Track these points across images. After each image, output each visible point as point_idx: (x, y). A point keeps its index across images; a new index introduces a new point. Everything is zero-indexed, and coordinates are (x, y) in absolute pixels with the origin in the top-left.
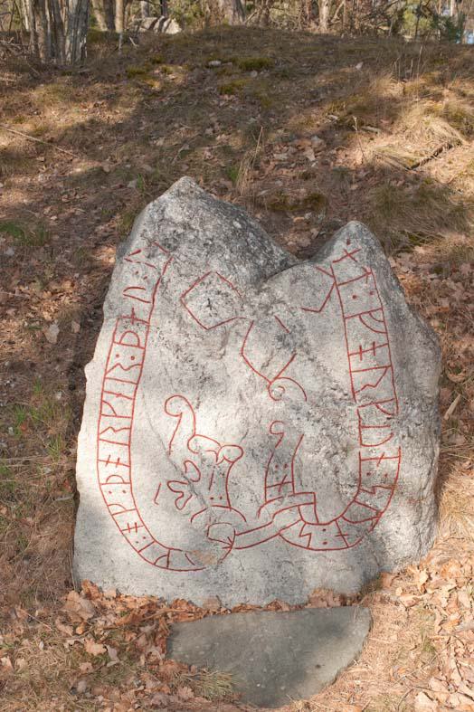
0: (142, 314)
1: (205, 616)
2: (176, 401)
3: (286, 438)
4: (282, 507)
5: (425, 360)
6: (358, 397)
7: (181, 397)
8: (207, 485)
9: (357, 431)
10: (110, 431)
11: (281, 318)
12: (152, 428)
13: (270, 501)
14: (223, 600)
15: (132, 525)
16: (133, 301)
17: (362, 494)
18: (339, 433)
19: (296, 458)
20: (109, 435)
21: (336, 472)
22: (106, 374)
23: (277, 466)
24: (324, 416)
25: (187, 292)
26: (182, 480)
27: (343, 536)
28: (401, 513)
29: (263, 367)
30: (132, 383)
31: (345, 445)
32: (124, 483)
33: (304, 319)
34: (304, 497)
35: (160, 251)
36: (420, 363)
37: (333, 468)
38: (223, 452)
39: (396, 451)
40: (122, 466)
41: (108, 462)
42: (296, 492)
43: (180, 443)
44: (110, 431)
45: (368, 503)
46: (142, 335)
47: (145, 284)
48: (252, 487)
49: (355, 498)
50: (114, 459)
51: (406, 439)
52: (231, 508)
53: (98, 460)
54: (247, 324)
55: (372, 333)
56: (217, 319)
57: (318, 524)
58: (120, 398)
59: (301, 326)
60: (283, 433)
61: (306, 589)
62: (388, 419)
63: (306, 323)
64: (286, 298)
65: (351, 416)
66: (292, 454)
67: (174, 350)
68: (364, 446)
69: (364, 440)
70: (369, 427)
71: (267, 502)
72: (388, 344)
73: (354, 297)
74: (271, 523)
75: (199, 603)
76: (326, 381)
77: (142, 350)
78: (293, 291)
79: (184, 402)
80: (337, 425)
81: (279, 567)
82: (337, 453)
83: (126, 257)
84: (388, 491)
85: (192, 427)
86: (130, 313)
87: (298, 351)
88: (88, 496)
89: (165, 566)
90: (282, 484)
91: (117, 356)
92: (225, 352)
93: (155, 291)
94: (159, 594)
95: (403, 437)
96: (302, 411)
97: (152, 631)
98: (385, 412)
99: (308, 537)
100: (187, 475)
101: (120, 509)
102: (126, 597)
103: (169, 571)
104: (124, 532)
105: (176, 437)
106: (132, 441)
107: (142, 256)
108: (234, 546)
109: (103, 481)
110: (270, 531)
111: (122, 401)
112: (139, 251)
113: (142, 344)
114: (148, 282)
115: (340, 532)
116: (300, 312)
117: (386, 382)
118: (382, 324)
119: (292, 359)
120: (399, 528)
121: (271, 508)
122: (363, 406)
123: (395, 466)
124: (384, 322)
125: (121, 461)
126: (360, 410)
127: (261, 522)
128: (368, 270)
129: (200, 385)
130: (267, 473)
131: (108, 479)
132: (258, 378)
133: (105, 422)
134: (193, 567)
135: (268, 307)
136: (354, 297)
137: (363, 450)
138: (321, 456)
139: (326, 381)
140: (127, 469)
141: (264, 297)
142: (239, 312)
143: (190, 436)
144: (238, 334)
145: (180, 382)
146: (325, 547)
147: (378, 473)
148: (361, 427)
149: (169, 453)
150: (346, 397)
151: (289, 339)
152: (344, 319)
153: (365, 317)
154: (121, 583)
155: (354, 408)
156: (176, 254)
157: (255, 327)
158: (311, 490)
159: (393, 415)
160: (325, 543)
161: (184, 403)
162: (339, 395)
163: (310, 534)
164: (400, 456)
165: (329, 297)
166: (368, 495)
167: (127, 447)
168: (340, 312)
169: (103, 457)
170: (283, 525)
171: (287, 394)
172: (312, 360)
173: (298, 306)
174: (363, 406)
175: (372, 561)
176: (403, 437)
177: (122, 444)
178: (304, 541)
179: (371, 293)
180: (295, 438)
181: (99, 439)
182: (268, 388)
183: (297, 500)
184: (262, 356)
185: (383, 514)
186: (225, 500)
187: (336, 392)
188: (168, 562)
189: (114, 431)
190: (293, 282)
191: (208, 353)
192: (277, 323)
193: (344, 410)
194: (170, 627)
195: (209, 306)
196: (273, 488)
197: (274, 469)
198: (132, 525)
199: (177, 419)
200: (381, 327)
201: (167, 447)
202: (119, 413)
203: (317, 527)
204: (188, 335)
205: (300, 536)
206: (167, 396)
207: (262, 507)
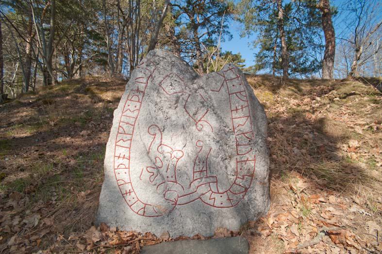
0: (142, 88)
1: (160, 243)
2: (154, 128)
4: (201, 183)
5: (263, 118)
6: (236, 131)
8: (165, 170)
9: (236, 147)
10: (121, 141)
11: (202, 94)
12: (141, 140)
13: (196, 180)
14: (171, 233)
15: (128, 191)
16: (139, 84)
17: (238, 179)
18: (227, 148)
19: (208, 159)
20: (121, 143)
21: (226, 168)
22: (123, 113)
23: (199, 162)
26: (154, 166)
27: (230, 200)
30: (134, 118)
31: (230, 154)
34: (211, 179)
35: (152, 64)
36: (260, 120)
38: (174, 154)
39: (253, 157)
40: (126, 159)
41: (119, 157)
43: (154, 148)
45: (241, 184)
46: (141, 97)
47: (144, 75)
51: (257, 152)
53: (115, 156)
54: (187, 95)
55: (241, 101)
56: (175, 91)
57: (218, 193)
58: (128, 125)
59: (210, 98)
60: (202, 146)
61: (213, 228)
62: (249, 141)
63: (213, 96)
64: (204, 86)
65: (233, 140)
66: (206, 157)
68: (239, 155)
69: (239, 152)
71: (194, 180)
73: (233, 86)
74: (196, 191)
75: (158, 235)
76: (222, 123)
79: (157, 128)
80: (227, 145)
81: (200, 215)
82: (226, 159)
83: (138, 66)
84: (250, 178)
85: (160, 141)
86: (137, 89)
87: (209, 109)
88: (108, 176)
90: (201, 171)
91: (129, 106)
93: (148, 79)
94: (139, 230)
96: (211, 137)
97: (130, 249)
98: (248, 138)
99: (213, 200)
100: (156, 164)
101: (123, 182)
102: (121, 231)
103: (144, 217)
106: (131, 146)
107: (144, 66)
108: (177, 203)
109: (116, 167)
110: (195, 196)
111: (128, 127)
113: (140, 101)
116: (210, 92)
117: (248, 123)
119: (207, 112)
120: (258, 196)
121: (196, 183)
123: (253, 165)
124: (246, 96)
125: (125, 156)
126: (237, 136)
127: (191, 190)
129: (165, 121)
131: (118, 166)
132: (191, 119)
133: (120, 136)
134: (157, 215)
135: (196, 90)
136: (233, 86)
137: (238, 157)
138: (219, 159)
141: (195, 86)
142: (184, 90)
143: (159, 145)
144: (183, 99)
145: (156, 119)
146: (222, 206)
147: (246, 168)
148: (237, 145)
149: (148, 153)
151: (205, 103)
153: (238, 94)
155: (234, 136)
156: (159, 66)
157: (191, 96)
160: (222, 204)
162: (227, 130)
163: (214, 198)
165: (223, 85)
166: (241, 180)
167: (128, 149)
168: (227, 91)
169: (117, 155)
170: (201, 192)
171: (204, 129)
172: (215, 114)
173: (209, 89)
175: (244, 214)
178: (211, 202)
179: (240, 85)
180: (208, 149)
181: (116, 145)
182: (196, 125)
183: (208, 180)
185: (248, 190)
186: (174, 178)
187: (226, 128)
188: (144, 212)
189: (124, 141)
192: (200, 96)
193: (229, 137)
194: (141, 248)
195: (171, 85)
197: (198, 163)
198: (128, 191)
199: (154, 136)
200: (245, 99)
201: (148, 149)
202: (126, 133)
204: (161, 98)
205: (210, 199)
206: (149, 125)
207: (192, 183)
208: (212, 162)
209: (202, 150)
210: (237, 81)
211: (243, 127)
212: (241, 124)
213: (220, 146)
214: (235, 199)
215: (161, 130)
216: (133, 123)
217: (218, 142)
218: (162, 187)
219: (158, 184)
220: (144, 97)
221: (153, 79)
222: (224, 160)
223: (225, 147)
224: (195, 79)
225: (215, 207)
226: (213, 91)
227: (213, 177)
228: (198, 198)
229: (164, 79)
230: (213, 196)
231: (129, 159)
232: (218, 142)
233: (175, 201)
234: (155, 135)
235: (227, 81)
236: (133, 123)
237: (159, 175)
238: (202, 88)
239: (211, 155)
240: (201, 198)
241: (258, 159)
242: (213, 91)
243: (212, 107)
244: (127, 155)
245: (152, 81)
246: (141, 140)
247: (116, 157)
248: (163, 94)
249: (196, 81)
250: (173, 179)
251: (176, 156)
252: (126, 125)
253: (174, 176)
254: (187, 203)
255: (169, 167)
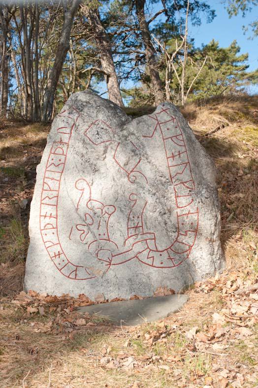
2: (81, 182)
3: (138, 202)
4: (137, 240)
5: (207, 165)
6: (174, 180)
7: (84, 179)
8: (97, 226)
9: (175, 199)
11: (133, 141)
12: (69, 196)
13: (131, 236)
15: (57, 253)
16: (61, 134)
17: (180, 236)
18: (166, 201)
19: (144, 214)
20: (47, 201)
22: (47, 168)
23: (133, 217)
24: (157, 192)
25: (87, 129)
26: (84, 223)
27: (171, 259)
28: (202, 246)
29: (125, 165)
30: (59, 172)
31: (169, 208)
32: (54, 228)
33: (144, 142)
34: (148, 235)
35: (74, 111)
37: (163, 221)
38: (105, 209)
41: (45, 216)
42: (144, 232)
44: (47, 199)
46: (65, 148)
48: (120, 229)
49: (177, 239)
50: (48, 215)
52: (110, 241)
54: (116, 144)
56: (102, 140)
57: (157, 251)
59: (143, 145)
60: (136, 200)
64: (135, 132)
67: (80, 156)
69: (178, 204)
70: (181, 196)
71: (129, 237)
72: (186, 151)
73: (168, 129)
77: (65, 156)
78: (138, 127)
80: (164, 197)
82: (165, 214)
84: (194, 233)
85: (89, 196)
86: (59, 140)
87: (142, 158)
89: (74, 277)
90: (136, 227)
91: (53, 159)
92: (105, 157)
93: (72, 128)
95: (199, 202)
96: (145, 189)
98: (188, 187)
101: (51, 244)
104: (53, 258)
105: (81, 200)
106: (58, 203)
107: (66, 113)
108: (112, 263)
109: (42, 228)
110: (131, 254)
111: (54, 182)
112: (65, 111)
113: (65, 154)
114: (69, 124)
115: (169, 256)
116: (142, 138)
117: (187, 171)
118: (182, 142)
122: (177, 185)
127: (126, 248)
128: (174, 117)
130: (128, 220)
132: (122, 170)
133: (45, 194)
134: (89, 276)
135: (126, 137)
136: (168, 129)
137: (178, 210)
138: (156, 214)
139: (157, 173)
140: (56, 219)
141: (125, 132)
142: (112, 138)
146: (162, 266)
148: (177, 197)
149: (77, 209)
150: (168, 180)
152: (164, 139)
153: (174, 139)
154: (50, 290)
155: (172, 187)
157: (120, 145)
158: (152, 231)
159: (192, 189)
160: (162, 263)
161: (85, 182)
163: (153, 257)
164: (198, 213)
165: (155, 129)
166: (183, 237)
167: (55, 207)
168: (161, 136)
172: (150, 162)
174: (177, 185)
176: (199, 202)
177: (53, 205)
178: (150, 261)
179: (176, 127)
181: (41, 203)
183: (145, 237)
184: (124, 159)
185: (193, 248)
186: (106, 236)
187: (162, 178)
188: (76, 275)
189: (50, 199)
190: (138, 124)
191: (97, 157)
192: (131, 144)
195: (98, 134)
196: (132, 229)
197: (132, 219)
200: (182, 143)
201: (76, 206)
203: (157, 252)
204: (87, 149)
205: (148, 258)
206: (77, 180)
208: (149, 217)
209: (137, 203)
210: (172, 124)
211: (182, 175)
212: (179, 172)
213: (157, 199)
214: (178, 258)
215: (90, 184)
216: (59, 179)
217: (154, 194)
218: (94, 245)
219: (89, 243)
220: (69, 149)
221: (77, 128)
222: (162, 215)
223: (162, 200)
224: (125, 124)
225: (155, 267)
226: (145, 137)
227: (150, 233)
228: (134, 257)
229: (89, 127)
230: (151, 254)
231: (57, 218)
232: (154, 194)
233: (109, 261)
234: (83, 190)
235: (161, 125)
236: (59, 179)
237: (90, 232)
238: (133, 134)
239: (146, 209)
240: (137, 257)
241: (202, 211)
242: (145, 137)
243: (146, 156)
244: (54, 214)
245: (76, 131)
246: (69, 196)
247: (41, 217)
248: (89, 144)
249: (125, 127)
250: (106, 237)
251: (107, 212)
252: (51, 181)
253: (106, 234)
254: (122, 263)
255: (101, 224)
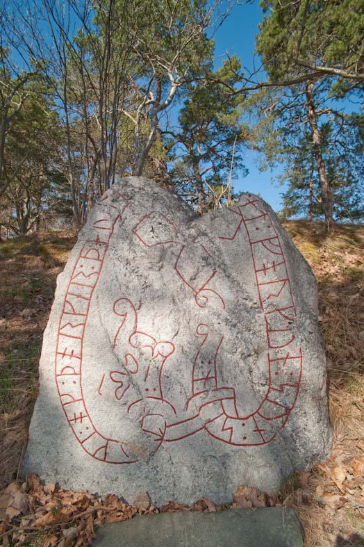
1: (133, 516)
3: (209, 338)
4: (206, 401)
5: (310, 284)
6: (265, 305)
7: (127, 299)
8: (143, 377)
9: (266, 334)
10: (69, 326)
11: (204, 245)
12: (102, 325)
13: (198, 394)
14: (152, 496)
15: (78, 415)
16: (99, 230)
17: (272, 392)
18: (251, 336)
19: (217, 357)
21: (250, 372)
23: (202, 362)
24: (239, 322)
25: (138, 224)
26: (123, 370)
27: (260, 431)
28: (307, 410)
29: (191, 279)
30: (90, 286)
31: (256, 348)
32: (75, 374)
33: (221, 246)
34: (225, 392)
35: (121, 198)
37: (247, 368)
38: (158, 348)
39: (298, 351)
41: (64, 354)
42: (218, 387)
43: (123, 337)
44: (69, 326)
45: (278, 400)
46: (102, 251)
48: (181, 380)
49: (267, 395)
50: (69, 352)
51: (304, 342)
52: (163, 400)
53: (57, 353)
54: (179, 246)
55: (272, 255)
56: (158, 240)
57: (238, 418)
58: (79, 299)
60: (207, 334)
61: (230, 486)
63: (223, 248)
64: (208, 231)
65: (260, 322)
66: (215, 353)
67: (124, 263)
69: (271, 343)
70: (275, 331)
71: (194, 395)
72: (284, 262)
73: (257, 229)
74: (197, 416)
75: (130, 500)
76: (240, 293)
77: (100, 262)
78: (212, 225)
81: (205, 461)
82: (249, 356)
84: (294, 389)
85: (133, 325)
87: (218, 269)
88: (46, 387)
89: (102, 457)
90: (207, 379)
91: (82, 266)
92: (162, 265)
93: (115, 222)
94: (94, 490)
95: (302, 340)
97: (74, 534)
99: (229, 431)
100: (127, 367)
101: (69, 399)
102: (64, 491)
103: (106, 464)
104: (72, 422)
105: (120, 332)
107: (108, 201)
108: (165, 438)
109: (58, 373)
110: (197, 424)
112: (107, 197)
113: (101, 258)
114: (111, 216)
115: (257, 427)
116: (217, 241)
117: (286, 291)
118: (279, 248)
119: (213, 275)
120: (309, 424)
121: (197, 401)
122: (269, 313)
124: (280, 246)
127: (189, 413)
128: (265, 213)
130: (194, 367)
132: (187, 288)
134: (127, 460)
135: (195, 238)
136: (257, 229)
137: (271, 352)
139: (240, 293)
140: (79, 360)
141: (193, 231)
142: (174, 238)
144: (172, 253)
145: (127, 287)
146: (245, 442)
147: (285, 371)
148: (269, 331)
149: (114, 346)
150: (255, 306)
151: (210, 260)
152: (251, 244)
153: (266, 243)
154: (63, 476)
155: (262, 315)
156: (132, 201)
158: (231, 386)
159: (293, 320)
161: (129, 304)
163: (231, 428)
164: (301, 357)
165: (239, 228)
166: (277, 393)
167: (80, 340)
168: (248, 238)
169: (61, 350)
170: (207, 418)
171: (210, 303)
173: (217, 236)
174: (269, 313)
175: (286, 457)
176: (302, 340)
177: (76, 338)
179: (269, 227)
181: (59, 334)
182: (195, 296)
183: (219, 395)
184: (191, 271)
185: (292, 411)
186: (158, 392)
187: (247, 302)
188: (106, 454)
189: (73, 327)
190: (212, 219)
191: (149, 265)
192: (201, 248)
193: (253, 318)
194: (96, 528)
195: (152, 231)
196: (199, 382)
197: (200, 365)
198: (78, 415)
199: (122, 318)
200: (278, 250)
201: (112, 340)
202: (77, 312)
203: (238, 421)
204: (135, 252)
205: (223, 430)
206: (116, 299)
207: (190, 399)
208: (225, 362)
209: (208, 339)
210: (263, 221)
211: (278, 298)
212: (273, 293)
213: (238, 333)
214: (269, 428)
215: (136, 307)
216: (88, 296)
217: (235, 326)
218: (137, 408)
219: (129, 404)
220: (108, 252)
221: (124, 222)
222: (245, 358)
223: (246, 334)
224: (193, 220)
225: (234, 444)
226: (223, 238)
227: (227, 388)
228: (201, 429)
229: (141, 221)
230: (229, 423)
231: (81, 359)
232: (235, 326)
233: (160, 433)
234: (126, 315)
235: (246, 222)
236: (88, 296)
237: (131, 386)
238: (205, 234)
239: (222, 348)
240: (206, 429)
241: (307, 354)
242: (223, 238)
243: (222, 266)
244: (77, 351)
245: (120, 226)
246: (102, 325)
248: (139, 245)
249: (193, 223)
250: (157, 394)
251: (161, 353)
252: (76, 300)
253: (158, 389)
254: (181, 438)
255: (150, 372)
